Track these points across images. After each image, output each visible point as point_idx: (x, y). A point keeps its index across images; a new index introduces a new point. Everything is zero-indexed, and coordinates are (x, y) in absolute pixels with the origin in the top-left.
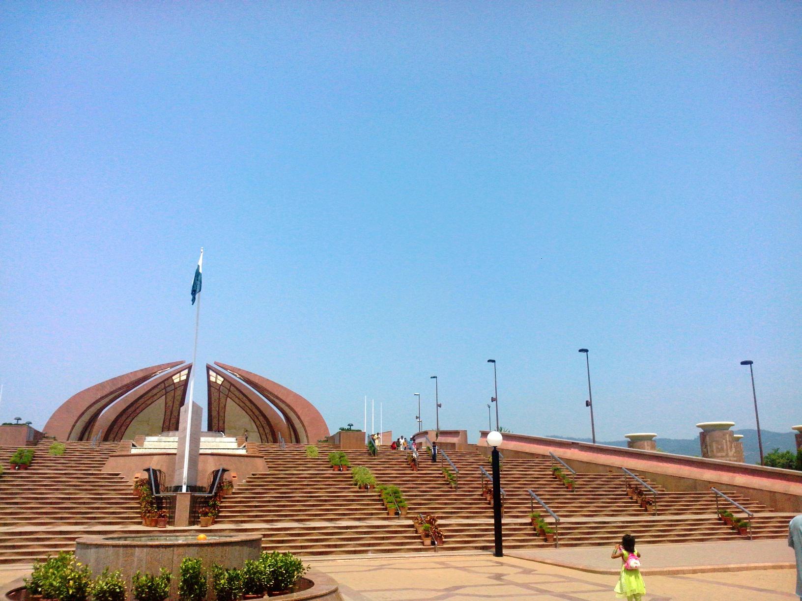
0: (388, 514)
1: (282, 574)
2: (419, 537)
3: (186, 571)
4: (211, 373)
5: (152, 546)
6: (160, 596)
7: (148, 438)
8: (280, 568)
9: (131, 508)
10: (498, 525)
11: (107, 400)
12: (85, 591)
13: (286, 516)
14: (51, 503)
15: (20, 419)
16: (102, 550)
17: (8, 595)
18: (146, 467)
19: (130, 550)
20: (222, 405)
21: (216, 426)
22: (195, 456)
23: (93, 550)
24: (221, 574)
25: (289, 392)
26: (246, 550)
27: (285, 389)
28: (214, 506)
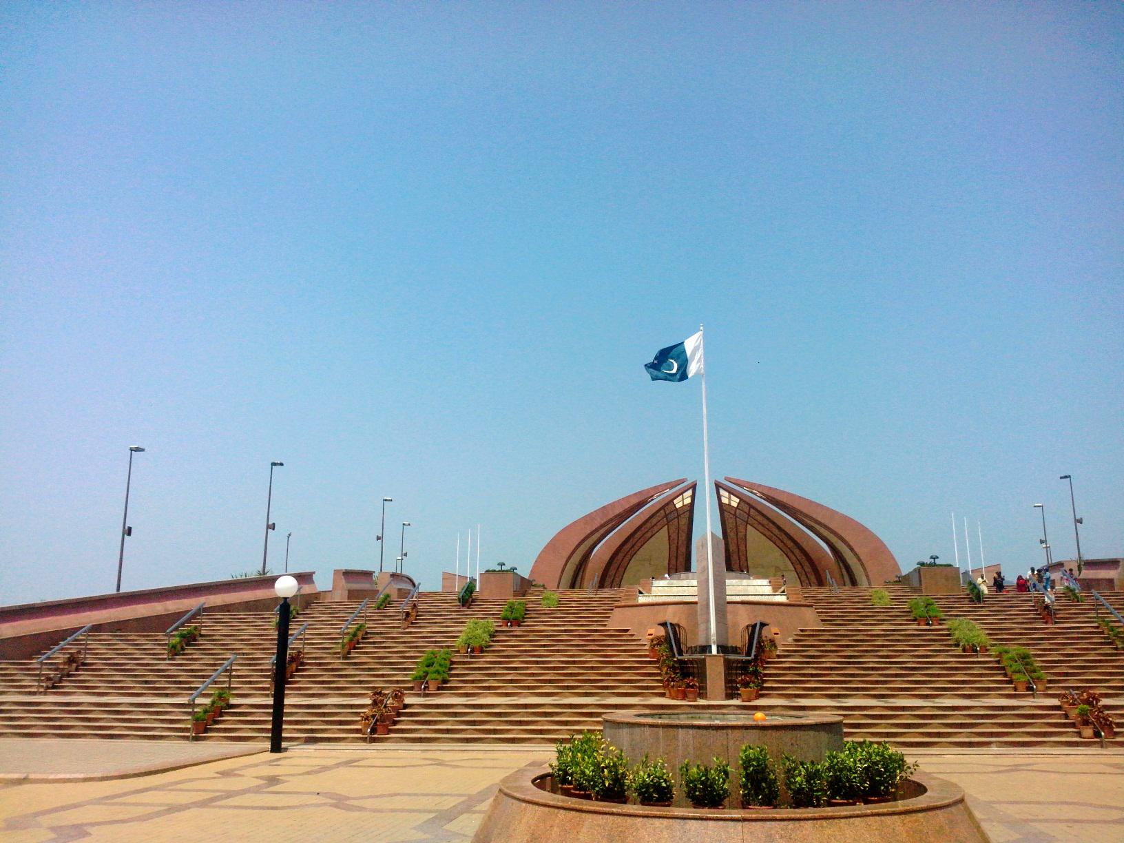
0: (1015, 689)
1: (880, 774)
2: (1073, 725)
3: (747, 763)
4: (722, 492)
5: (699, 727)
6: (719, 795)
8: (876, 763)
11: (597, 535)
12: (623, 785)
13: (857, 689)
14: (554, 668)
16: (637, 730)
17: (533, 781)
18: (661, 620)
19: (672, 732)
20: (741, 535)
22: (723, 605)
23: (625, 731)
24: (795, 769)
25: (834, 513)
26: (824, 737)
27: (828, 509)
28: (756, 673)
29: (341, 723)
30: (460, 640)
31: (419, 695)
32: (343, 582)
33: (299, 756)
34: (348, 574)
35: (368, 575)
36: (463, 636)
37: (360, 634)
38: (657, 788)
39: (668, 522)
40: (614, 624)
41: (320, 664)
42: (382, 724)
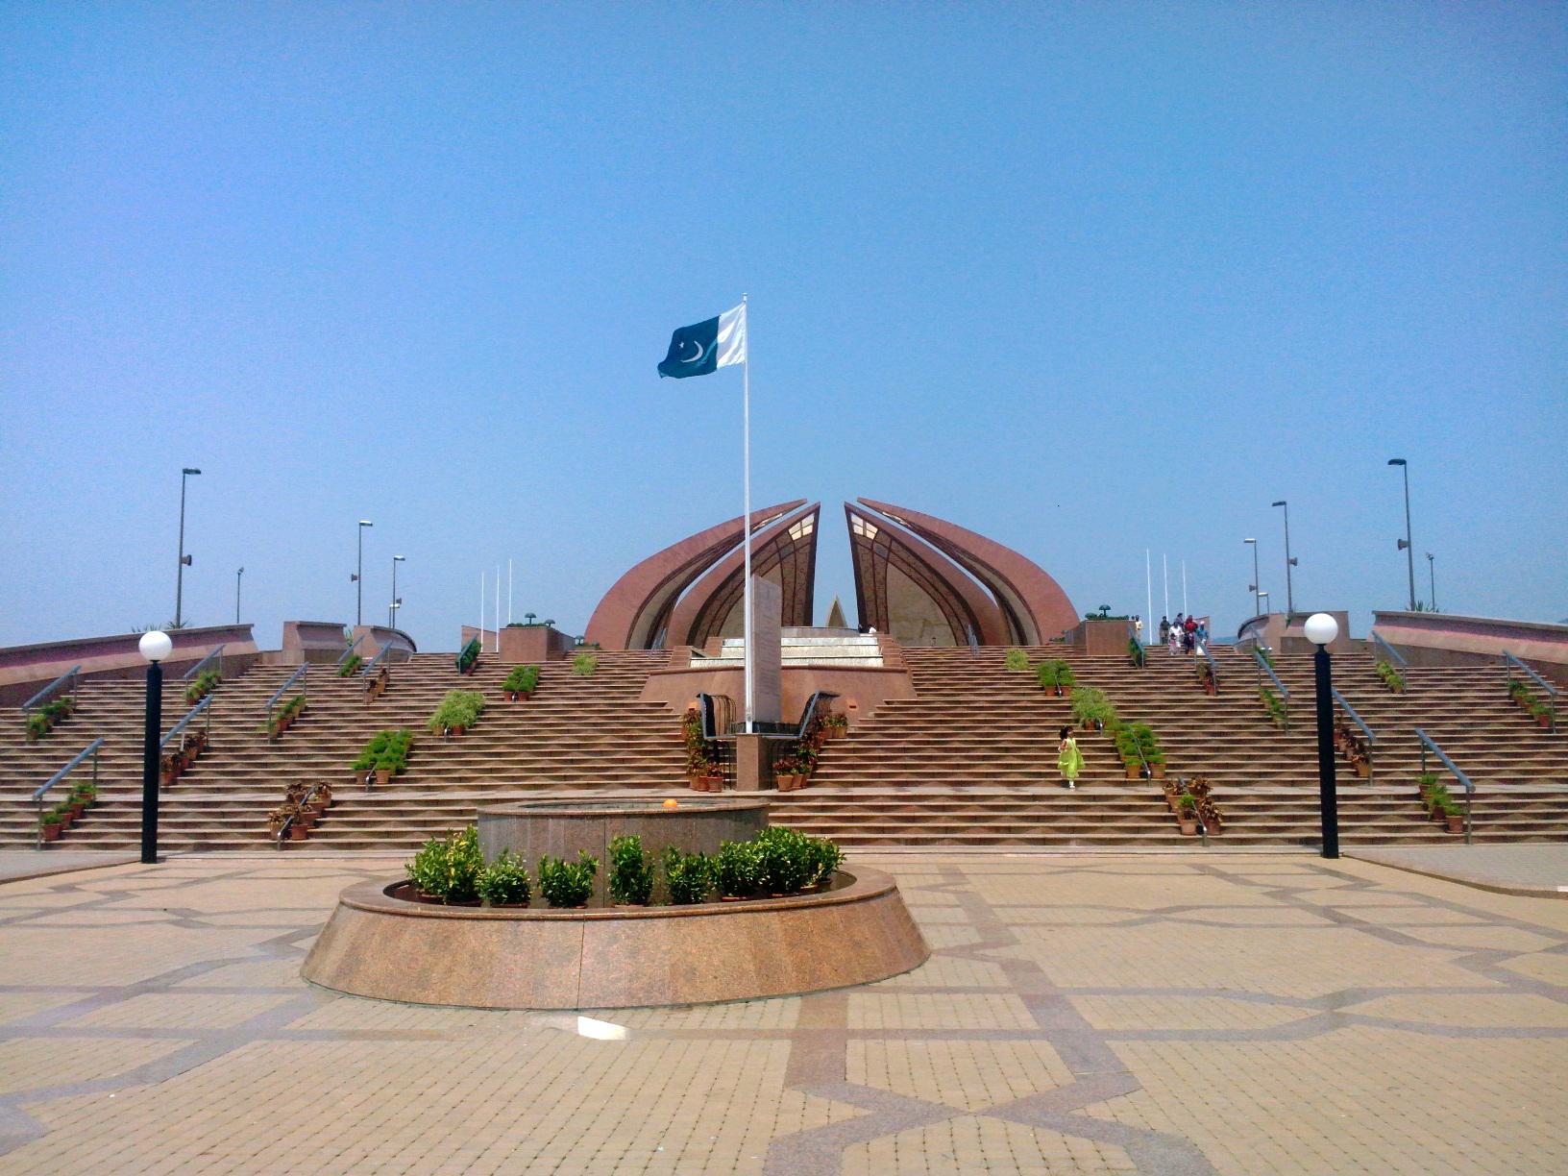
0: (1127, 775)
2: (1174, 819)
4: (854, 518)
5: (572, 817)
7: (730, 642)
9: (675, 760)
10: (1329, 803)
11: (682, 577)
13: (933, 775)
14: (551, 754)
16: (505, 822)
20: (879, 577)
27: (991, 543)
28: (806, 757)
29: (244, 825)
30: (433, 718)
31: (362, 789)
33: (179, 865)
34: (303, 627)
35: (336, 629)
36: (438, 713)
37: (297, 710)
38: (507, 885)
39: (781, 560)
40: (647, 697)
41: (231, 750)
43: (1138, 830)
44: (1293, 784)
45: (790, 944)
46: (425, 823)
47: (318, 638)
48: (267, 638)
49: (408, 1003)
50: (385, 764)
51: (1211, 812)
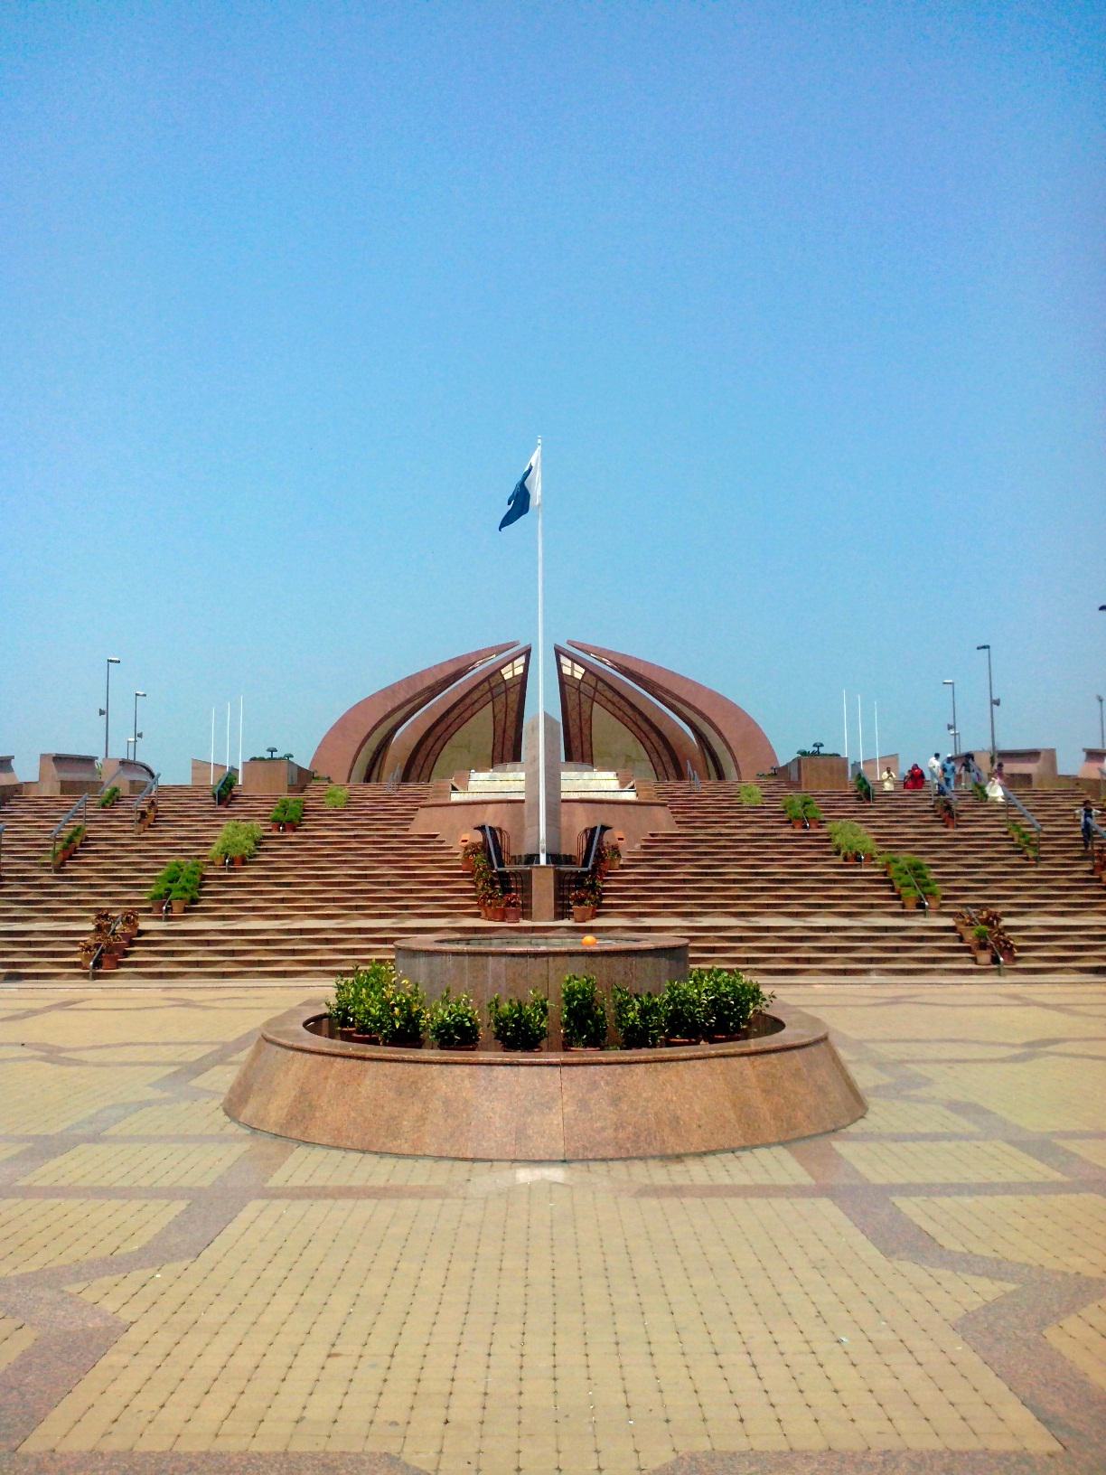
0: (903, 906)
1: (730, 1008)
4: (564, 660)
5: (513, 954)
6: (534, 1035)
8: (726, 995)
9: (461, 891)
12: (418, 1025)
13: (715, 906)
14: (339, 884)
15: (272, 751)
16: (437, 960)
17: (305, 1025)
18: (479, 824)
20: (585, 716)
21: (578, 749)
22: (557, 804)
23: (423, 960)
24: (628, 1002)
26: (664, 963)
27: (694, 683)
28: (593, 888)
29: (53, 954)
31: (159, 919)
32: (55, 773)
34: (60, 760)
35: (88, 761)
37: (78, 840)
38: (459, 1027)
40: (418, 828)
41: (24, 879)
42: (108, 955)
43: (934, 960)
44: (1062, 914)
45: (763, 1091)
46: (233, 953)
47: (72, 769)
48: (26, 770)
49: (381, 1154)
50: (180, 894)
51: (1006, 942)
